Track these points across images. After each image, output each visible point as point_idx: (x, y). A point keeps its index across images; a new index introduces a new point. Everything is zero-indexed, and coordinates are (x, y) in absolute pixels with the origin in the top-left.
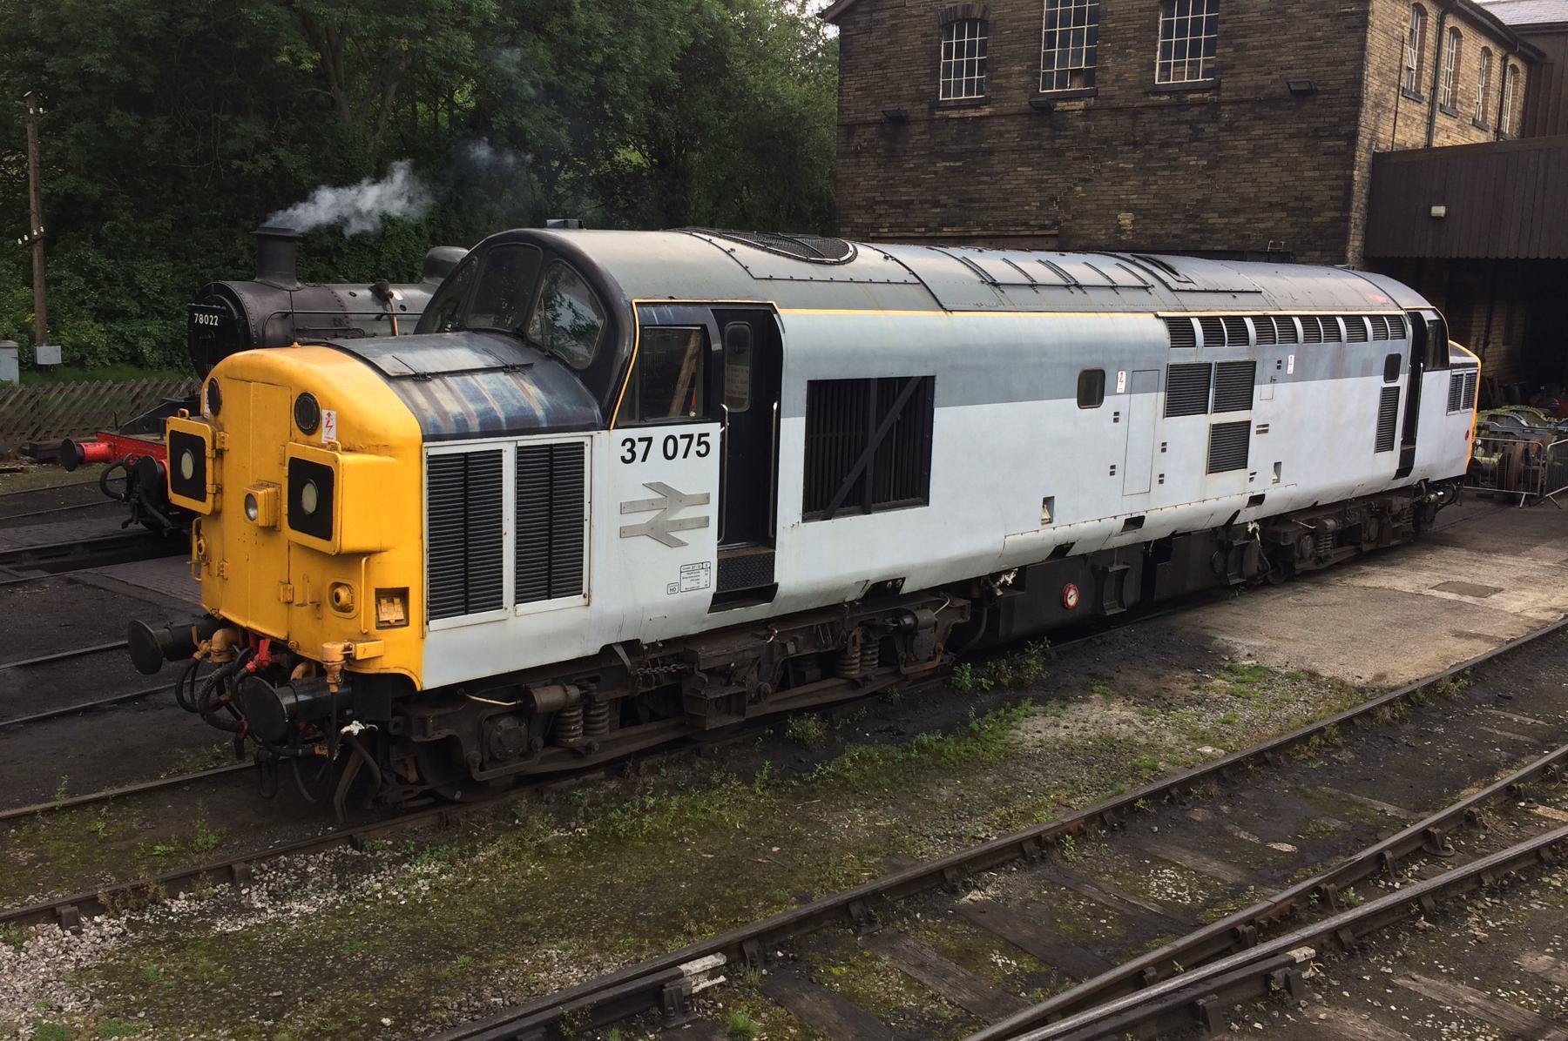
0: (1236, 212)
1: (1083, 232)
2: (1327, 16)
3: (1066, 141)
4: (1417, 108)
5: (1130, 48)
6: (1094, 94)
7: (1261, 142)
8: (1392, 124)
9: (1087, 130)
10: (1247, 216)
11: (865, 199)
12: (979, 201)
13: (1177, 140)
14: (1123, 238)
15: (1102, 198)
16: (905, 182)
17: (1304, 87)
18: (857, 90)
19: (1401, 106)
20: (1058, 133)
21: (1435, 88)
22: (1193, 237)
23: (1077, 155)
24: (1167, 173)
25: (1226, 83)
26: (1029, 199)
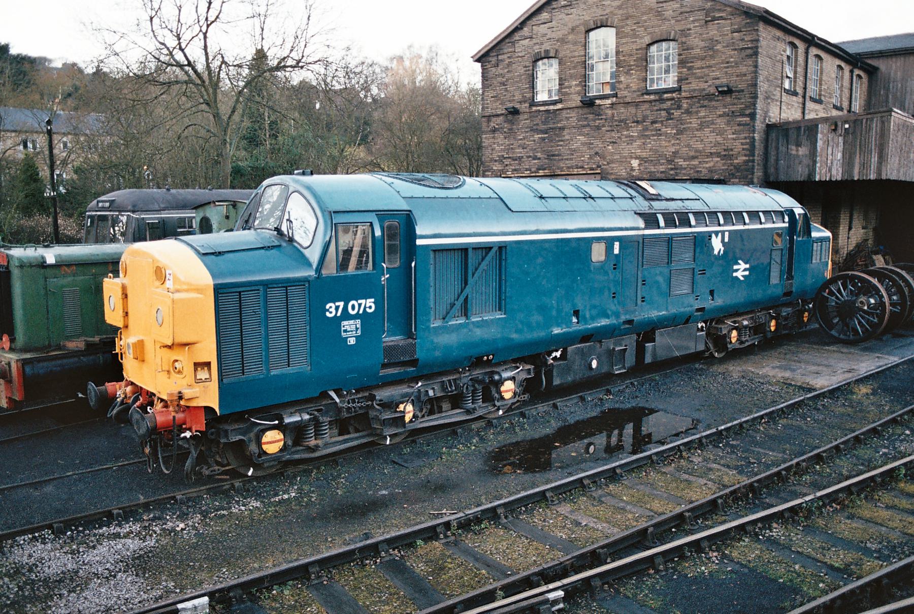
0: (694, 158)
2: (735, 50)
4: (794, 98)
5: (632, 70)
6: (616, 95)
8: (778, 108)
10: (701, 160)
11: (499, 156)
14: (634, 174)
17: (726, 89)
18: (492, 97)
19: (784, 98)
21: (805, 88)
23: (609, 128)
25: (684, 88)
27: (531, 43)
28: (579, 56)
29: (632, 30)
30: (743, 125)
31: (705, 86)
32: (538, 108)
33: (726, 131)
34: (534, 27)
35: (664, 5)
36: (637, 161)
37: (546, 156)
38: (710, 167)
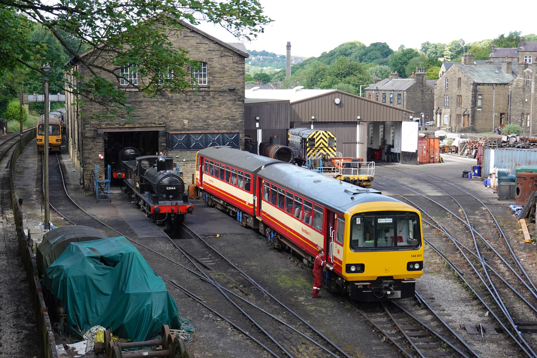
0: (216, 120)
14: (185, 127)
23: (170, 103)
30: (240, 105)
35: (200, 45)
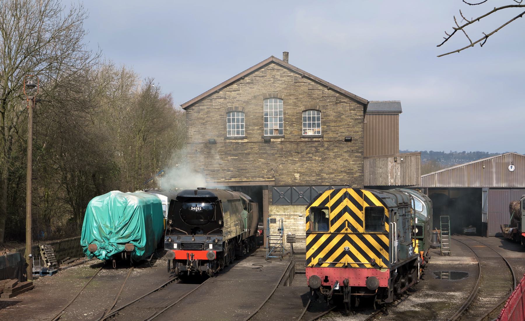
0: (332, 173)
1: (284, 180)
2: (353, 119)
3: (275, 151)
5: (294, 124)
6: (283, 137)
7: (337, 153)
9: (282, 149)
12: (244, 170)
13: (312, 152)
14: (297, 181)
15: (288, 169)
16: (216, 163)
18: (194, 132)
20: (272, 148)
22: (319, 181)
24: (309, 162)
26: (263, 169)
27: (225, 101)
28: (259, 113)
29: (293, 102)
31: (337, 136)
32: (230, 141)
33: (349, 160)
34: (227, 92)
35: (312, 91)
36: (299, 174)
37: (237, 170)
38: (341, 178)
